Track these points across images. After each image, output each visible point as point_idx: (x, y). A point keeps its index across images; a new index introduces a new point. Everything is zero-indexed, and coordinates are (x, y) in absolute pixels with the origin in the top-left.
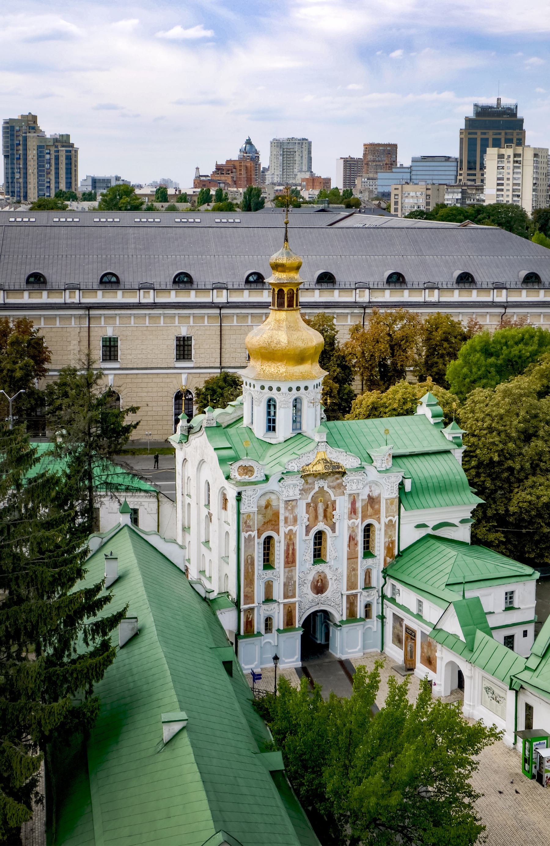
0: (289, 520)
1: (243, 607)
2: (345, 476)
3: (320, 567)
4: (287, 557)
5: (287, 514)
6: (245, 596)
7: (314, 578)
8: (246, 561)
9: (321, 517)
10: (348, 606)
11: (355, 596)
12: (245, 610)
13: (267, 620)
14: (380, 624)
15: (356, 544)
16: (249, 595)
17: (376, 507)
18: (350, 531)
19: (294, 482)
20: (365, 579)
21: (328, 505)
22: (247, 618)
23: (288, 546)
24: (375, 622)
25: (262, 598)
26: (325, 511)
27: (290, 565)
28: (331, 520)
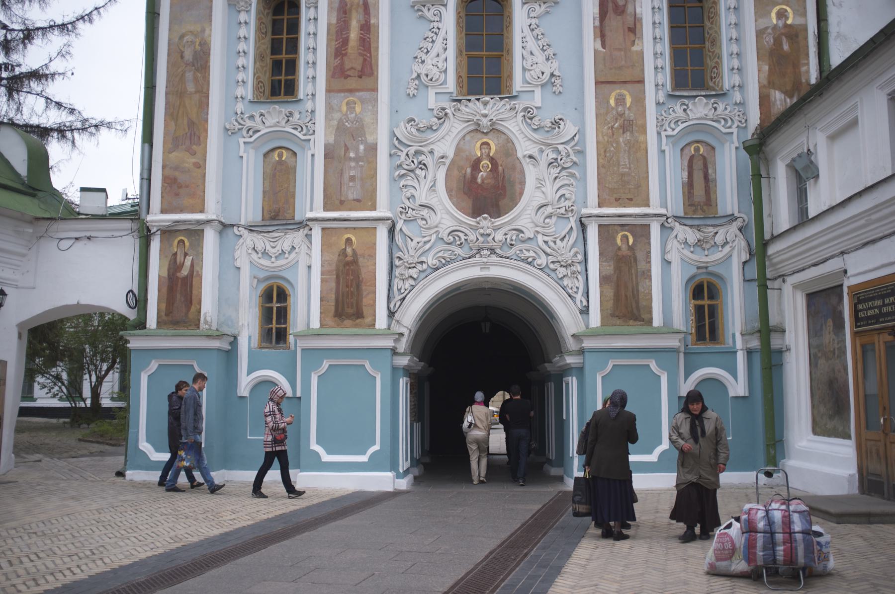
1: (156, 217)
3: (489, 109)
4: (339, 48)
6: (169, 182)
7: (458, 150)
8: (176, 53)
10: (610, 269)
11: (642, 232)
12: (168, 233)
13: (267, 296)
15: (634, 29)
16: (182, 178)
20: (689, 186)
22: (174, 267)
24: (741, 358)
25: (250, 209)
27: (352, 83)
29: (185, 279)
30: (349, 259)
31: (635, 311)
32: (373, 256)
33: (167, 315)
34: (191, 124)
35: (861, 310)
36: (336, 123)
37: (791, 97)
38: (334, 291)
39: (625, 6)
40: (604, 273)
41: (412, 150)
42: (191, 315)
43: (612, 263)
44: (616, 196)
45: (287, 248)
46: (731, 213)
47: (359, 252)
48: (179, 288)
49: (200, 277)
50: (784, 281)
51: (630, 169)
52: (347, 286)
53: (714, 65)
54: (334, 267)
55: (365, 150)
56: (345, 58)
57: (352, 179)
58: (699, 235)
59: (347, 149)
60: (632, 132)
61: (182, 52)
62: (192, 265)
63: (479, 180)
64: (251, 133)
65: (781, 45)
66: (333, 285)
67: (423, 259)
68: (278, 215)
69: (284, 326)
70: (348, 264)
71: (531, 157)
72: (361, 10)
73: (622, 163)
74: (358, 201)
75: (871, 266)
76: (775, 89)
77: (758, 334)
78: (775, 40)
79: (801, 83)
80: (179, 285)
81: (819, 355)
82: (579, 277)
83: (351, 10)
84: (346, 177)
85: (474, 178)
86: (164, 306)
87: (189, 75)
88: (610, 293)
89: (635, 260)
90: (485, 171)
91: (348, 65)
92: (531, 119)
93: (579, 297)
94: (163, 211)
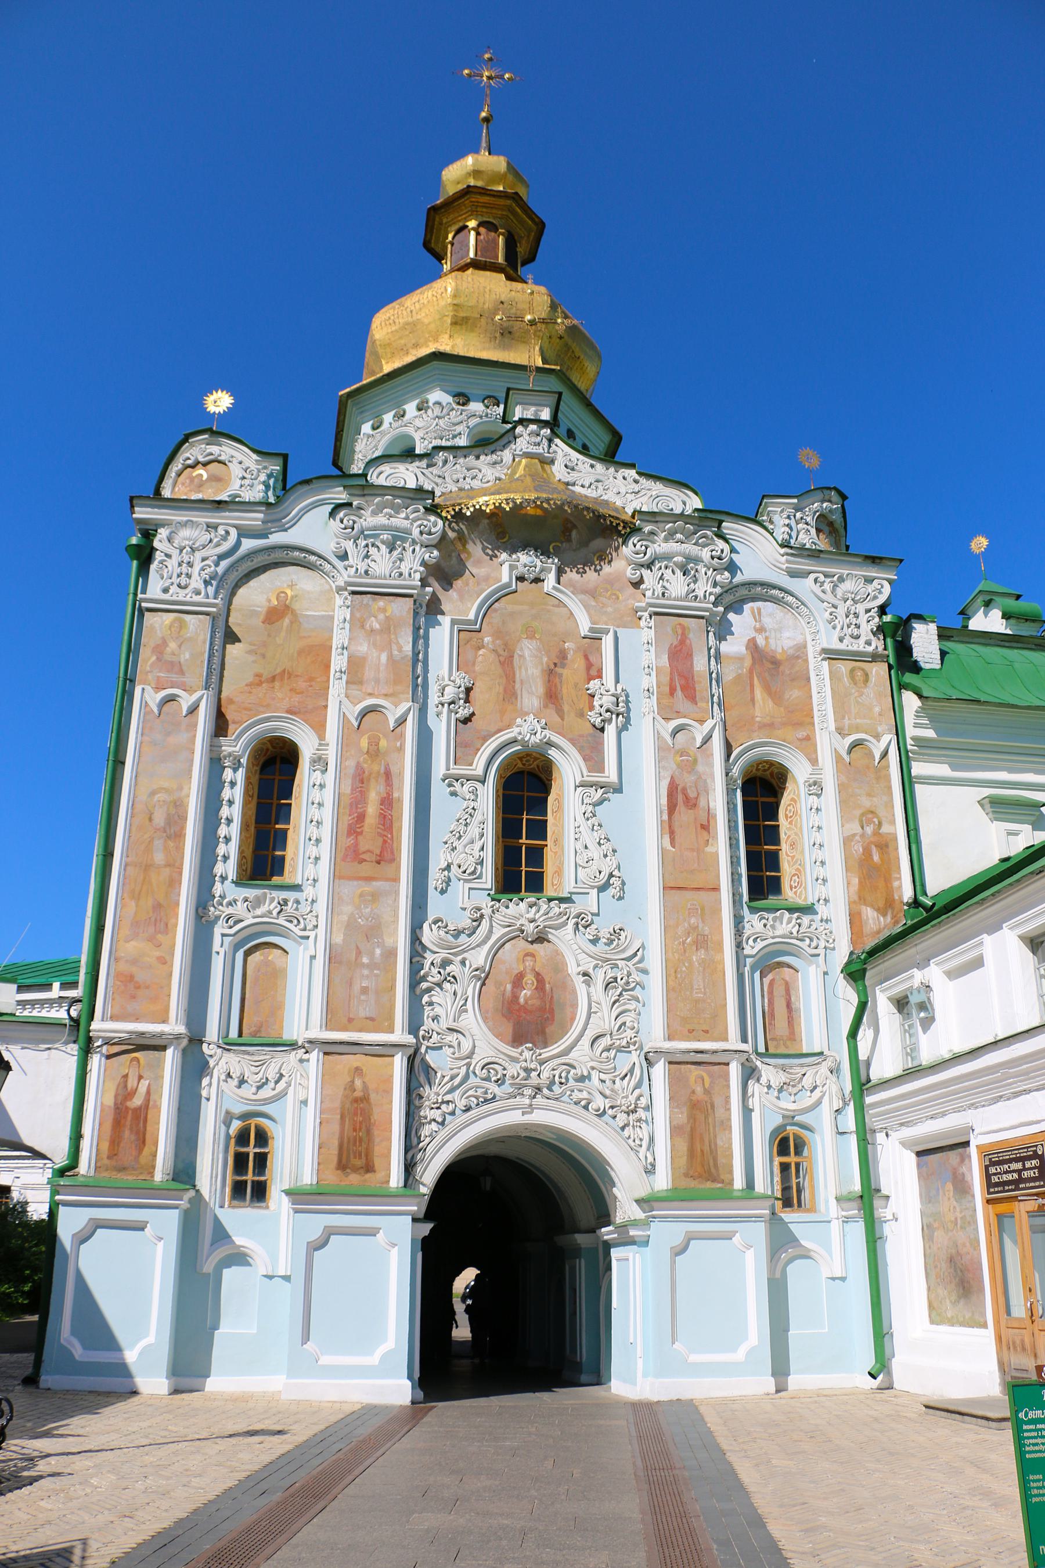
0: (369, 674)
2: (634, 539)
5: (363, 648)
9: (531, 697)
10: (682, 1118)
13: (242, 1138)
14: (859, 1228)
15: (706, 827)
16: (140, 976)
17: (794, 694)
18: (671, 766)
19: (399, 521)
21: (563, 655)
23: (361, 779)
26: (551, 674)
27: (366, 869)
28: (582, 715)
29: (137, 1111)
30: (358, 1094)
31: (713, 1170)
32: (389, 1092)
33: (109, 1158)
34: (158, 906)
35: (995, 1174)
36: (345, 918)
37: (884, 915)
38: (337, 1136)
39: (697, 798)
40: (675, 1123)
41: (438, 959)
42: (143, 1159)
43: (685, 1109)
44: (689, 1027)
45: (272, 1075)
46: (817, 1050)
47: (372, 1086)
48: (128, 1123)
49: (158, 1109)
50: (887, 1135)
51: (705, 994)
52: (355, 1130)
53: (794, 872)
54: (337, 1104)
55: (382, 955)
56: (360, 838)
57: (365, 990)
58: (783, 1077)
59: (359, 953)
60: (707, 949)
61: (152, 814)
62: (148, 1093)
63: (522, 1000)
64: (231, 922)
65: (871, 855)
66: (336, 1127)
67: (447, 1098)
68: (259, 1031)
69: (262, 1178)
70: (356, 1100)
71: (585, 974)
72: (382, 780)
73: (696, 987)
74: (372, 1019)
75: (1007, 1125)
76: (866, 905)
77: (859, 1201)
78: (864, 849)
79: (894, 900)
80: (129, 1118)
81: (936, 1225)
82: (644, 1125)
83: (369, 780)
84: (356, 988)
85: (515, 997)
86: (105, 1146)
87: (158, 843)
88: (683, 1146)
89: (713, 1106)
90: (529, 989)
91: (363, 847)
92: (586, 927)
93: (643, 1151)
94: (113, 1018)
